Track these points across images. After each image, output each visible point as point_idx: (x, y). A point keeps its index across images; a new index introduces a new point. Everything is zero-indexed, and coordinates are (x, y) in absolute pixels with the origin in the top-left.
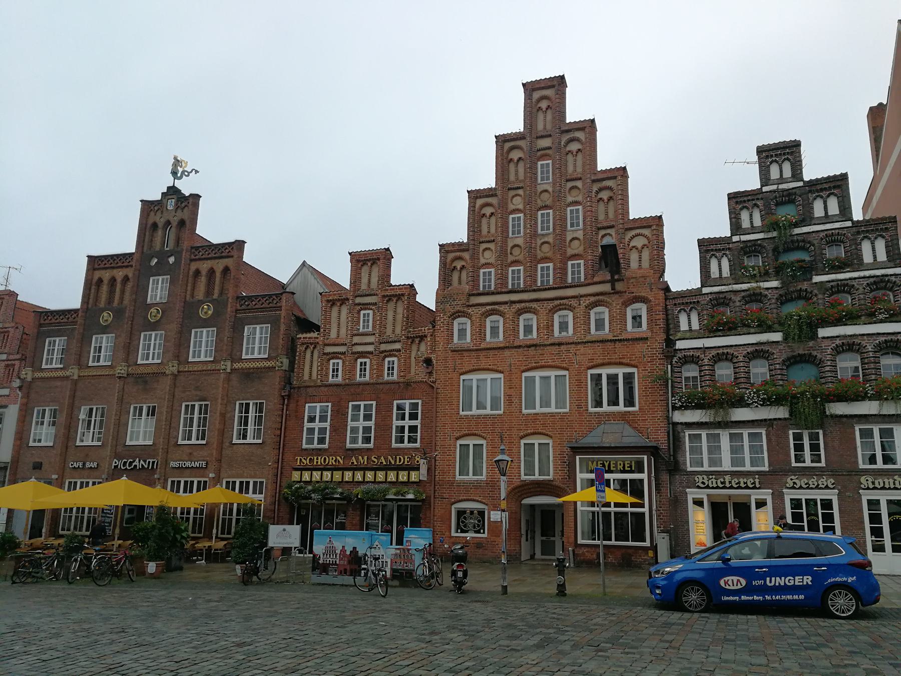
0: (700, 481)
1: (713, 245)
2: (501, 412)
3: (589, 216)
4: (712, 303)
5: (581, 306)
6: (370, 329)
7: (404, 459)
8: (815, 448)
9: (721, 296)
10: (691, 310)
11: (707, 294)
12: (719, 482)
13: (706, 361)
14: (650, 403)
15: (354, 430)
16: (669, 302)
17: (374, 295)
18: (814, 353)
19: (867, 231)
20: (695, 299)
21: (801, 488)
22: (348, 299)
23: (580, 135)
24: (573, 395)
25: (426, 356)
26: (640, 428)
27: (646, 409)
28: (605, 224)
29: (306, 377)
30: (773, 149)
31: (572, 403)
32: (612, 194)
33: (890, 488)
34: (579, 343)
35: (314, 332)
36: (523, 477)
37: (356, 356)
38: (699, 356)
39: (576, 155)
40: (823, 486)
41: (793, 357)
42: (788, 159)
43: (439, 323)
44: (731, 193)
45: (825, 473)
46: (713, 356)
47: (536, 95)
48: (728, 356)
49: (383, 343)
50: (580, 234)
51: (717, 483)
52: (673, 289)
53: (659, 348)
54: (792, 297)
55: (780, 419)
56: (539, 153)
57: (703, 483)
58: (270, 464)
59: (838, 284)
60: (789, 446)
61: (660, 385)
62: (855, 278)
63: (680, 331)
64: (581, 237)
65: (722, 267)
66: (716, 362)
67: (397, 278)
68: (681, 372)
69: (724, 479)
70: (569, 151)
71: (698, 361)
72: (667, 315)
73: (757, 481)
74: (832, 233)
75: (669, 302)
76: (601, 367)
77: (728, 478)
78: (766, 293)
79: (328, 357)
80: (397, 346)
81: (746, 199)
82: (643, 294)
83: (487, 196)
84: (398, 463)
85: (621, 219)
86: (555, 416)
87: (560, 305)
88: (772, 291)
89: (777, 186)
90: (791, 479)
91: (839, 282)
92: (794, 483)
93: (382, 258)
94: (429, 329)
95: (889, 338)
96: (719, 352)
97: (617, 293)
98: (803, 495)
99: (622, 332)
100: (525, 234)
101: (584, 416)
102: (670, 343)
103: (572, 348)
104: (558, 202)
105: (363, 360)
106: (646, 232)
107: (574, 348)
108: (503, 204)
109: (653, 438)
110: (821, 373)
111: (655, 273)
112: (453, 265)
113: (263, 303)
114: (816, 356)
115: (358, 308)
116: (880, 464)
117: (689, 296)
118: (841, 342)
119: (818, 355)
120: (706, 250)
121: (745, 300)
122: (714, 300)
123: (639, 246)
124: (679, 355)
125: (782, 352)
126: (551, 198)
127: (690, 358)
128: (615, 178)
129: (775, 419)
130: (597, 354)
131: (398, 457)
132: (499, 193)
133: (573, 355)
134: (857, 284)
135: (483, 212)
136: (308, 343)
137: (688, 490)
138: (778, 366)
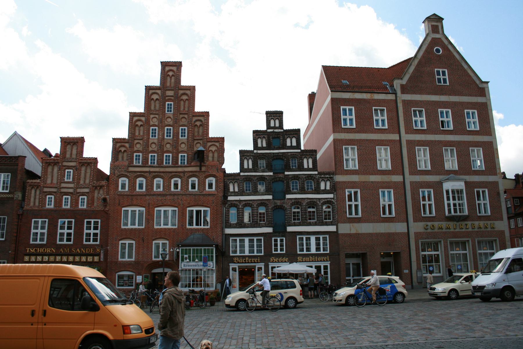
2: (143, 227)
6: (71, 180)
7: (91, 250)
8: (282, 245)
10: (235, 182)
11: (242, 176)
12: (243, 260)
13: (241, 206)
15: (62, 234)
17: (74, 162)
18: (284, 205)
19: (306, 155)
21: (276, 262)
22: (58, 163)
23: (188, 92)
25: (103, 196)
28: (198, 138)
29: (32, 204)
33: (308, 261)
35: (37, 179)
36: (154, 259)
37: (63, 194)
41: (276, 206)
42: (278, 119)
43: (111, 179)
47: (167, 68)
49: (79, 188)
51: (242, 261)
52: (227, 172)
55: (269, 233)
56: (167, 98)
57: (237, 261)
58: (10, 252)
65: (249, 164)
66: (244, 207)
67: (87, 153)
68: (229, 211)
69: (246, 259)
70: (182, 99)
73: (259, 259)
77: (247, 259)
78: (267, 177)
79: (46, 194)
80: (87, 190)
82: (214, 173)
83: (139, 116)
84: (87, 252)
87: (175, 175)
93: (79, 142)
94: (105, 183)
95: (311, 200)
97: (202, 172)
100: (158, 138)
102: (225, 197)
103: (180, 197)
104: (176, 123)
105: (67, 197)
106: (217, 144)
108: (147, 122)
112: (120, 149)
113: (6, 161)
115: (64, 168)
116: (305, 252)
124: (229, 203)
126: (172, 121)
127: (234, 204)
128: (203, 116)
129: (267, 233)
131: (87, 249)
132: (146, 115)
135: (137, 123)
136: (33, 185)
137: (230, 264)
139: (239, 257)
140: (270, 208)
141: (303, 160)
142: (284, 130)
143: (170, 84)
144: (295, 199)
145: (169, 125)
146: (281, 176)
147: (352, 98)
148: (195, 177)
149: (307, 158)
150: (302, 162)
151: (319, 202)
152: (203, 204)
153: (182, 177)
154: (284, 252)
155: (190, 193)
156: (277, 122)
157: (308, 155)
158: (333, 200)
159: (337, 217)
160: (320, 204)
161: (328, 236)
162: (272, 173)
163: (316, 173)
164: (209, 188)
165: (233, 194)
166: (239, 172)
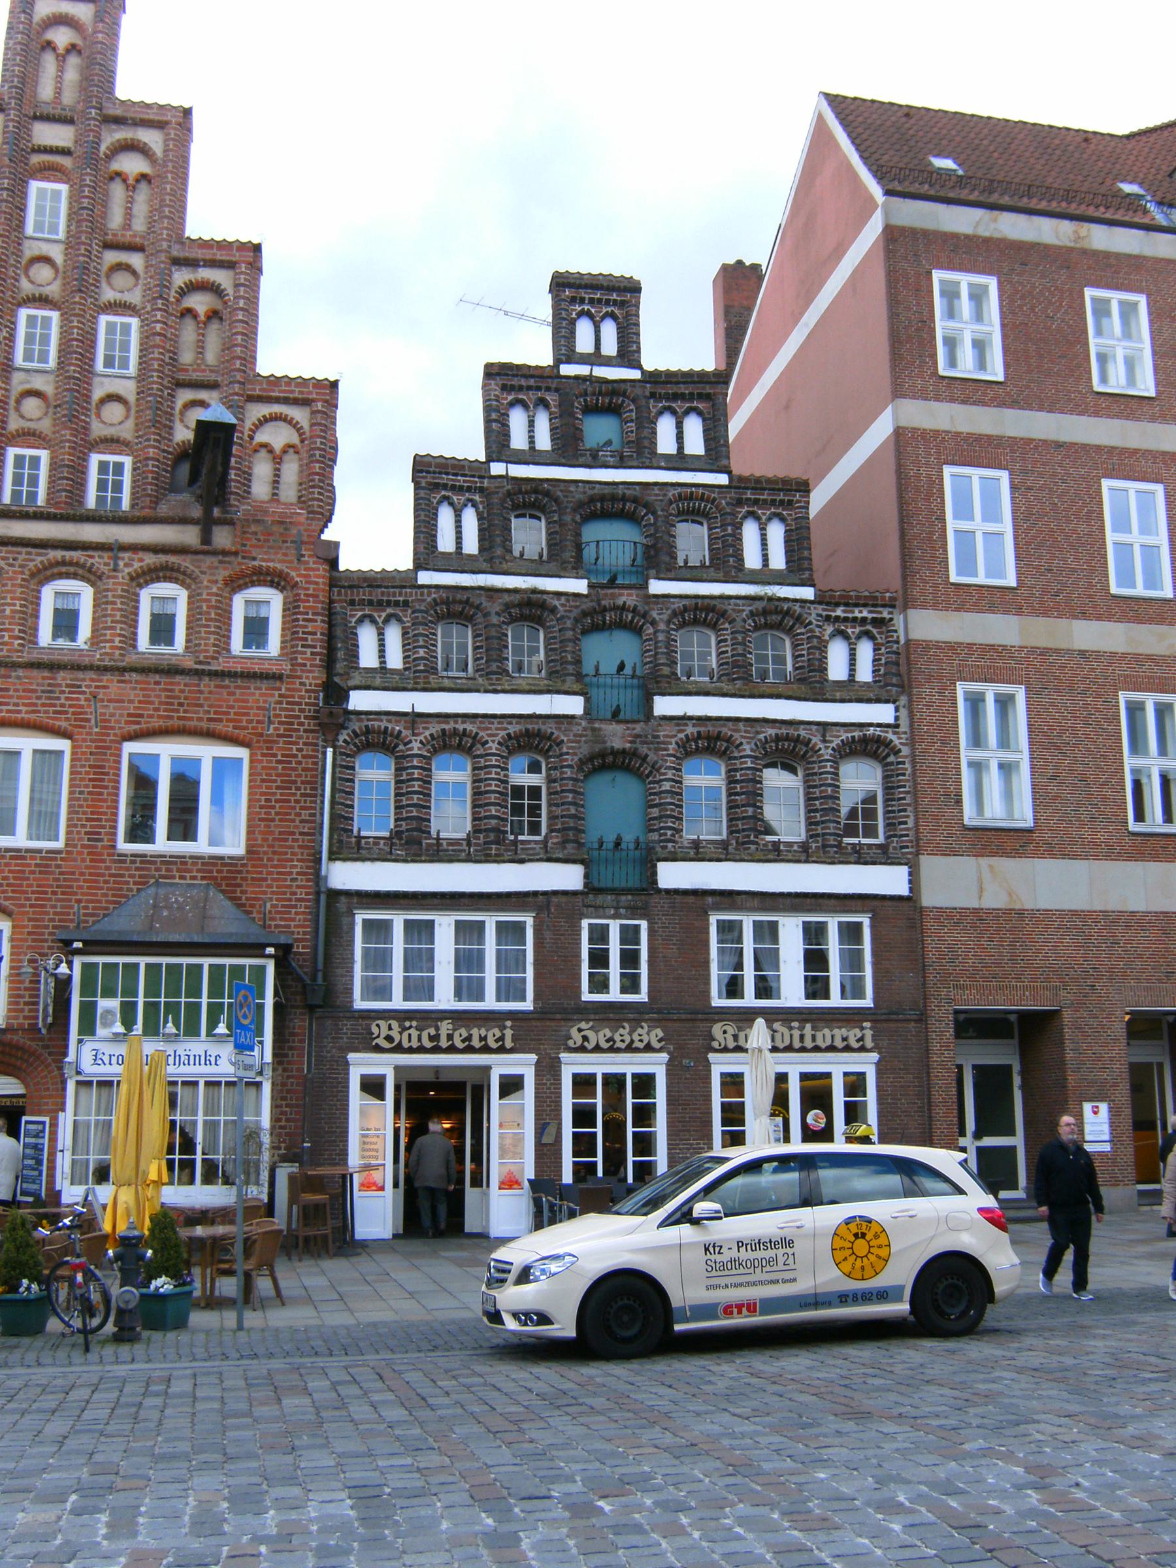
0: (383, 1035)
1: (447, 474)
3: (158, 346)
4: (436, 611)
5: (120, 575)
8: (630, 959)
9: (459, 597)
10: (387, 621)
12: (425, 1035)
13: (416, 745)
14: (274, 839)
16: (339, 594)
18: (643, 750)
19: (756, 502)
20: (400, 594)
21: (597, 1049)
23: (152, 138)
24: (81, 806)
26: (247, 899)
27: (265, 853)
28: (195, 376)
30: (586, 287)
31: (75, 826)
32: (219, 306)
34: (106, 669)
38: (400, 732)
39: (134, 187)
40: (641, 1045)
41: (602, 755)
42: (613, 316)
44: (492, 364)
45: (647, 1017)
46: (431, 735)
48: (465, 739)
50: (128, 389)
51: (420, 1040)
52: (348, 562)
53: (306, 704)
54: (604, 621)
55: (565, 893)
56: (36, 159)
57: (389, 1039)
59: (697, 604)
60: (578, 956)
61: (302, 795)
62: (730, 597)
63: (358, 668)
64: (132, 398)
66: (435, 751)
68: (353, 768)
69: (437, 1029)
70: (118, 174)
71: (397, 745)
72: (331, 625)
73: (509, 1033)
74: (692, 493)
75: (339, 594)
76: (160, 739)
77: (445, 1027)
78: (556, 603)
81: (523, 382)
82: (279, 566)
85: (239, 370)
86: (24, 858)
87: (63, 563)
88: (568, 601)
89: (589, 367)
90: (580, 1030)
91: (700, 601)
92: (585, 1038)
95: (784, 731)
96: (446, 727)
98: (599, 1066)
99: (218, 652)
101: (103, 861)
102: (336, 693)
103: (87, 680)
106: (299, 414)
107: (92, 680)
109: (276, 926)
110: (651, 794)
111: (312, 519)
114: (647, 756)
117: (387, 587)
118: (695, 730)
119: (652, 757)
120: (430, 484)
121: (510, 614)
122: (442, 603)
123: (278, 445)
124: (356, 726)
125: (579, 742)
126: (58, 282)
128: (230, 265)
129: (555, 893)
130: (152, 703)
133: (86, 700)
134: (733, 610)
137: (352, 1056)
138: (568, 773)
139: (403, 1016)
140: (570, 760)
141: (739, 526)
142: (643, 372)
143: (58, 91)
144: (699, 719)
145: (42, 301)
146: (629, 598)
147: (987, 234)
148: (175, 580)
149: (757, 518)
150: (733, 535)
151: (824, 741)
152: (212, 725)
153: (100, 578)
154: (643, 996)
155: (146, 663)
156: (609, 331)
157: (765, 501)
158: (890, 736)
159: (911, 824)
160: (827, 753)
161: (865, 921)
162: (585, 582)
163: (808, 593)
164: (247, 645)
165: (378, 681)
166: (411, 567)
